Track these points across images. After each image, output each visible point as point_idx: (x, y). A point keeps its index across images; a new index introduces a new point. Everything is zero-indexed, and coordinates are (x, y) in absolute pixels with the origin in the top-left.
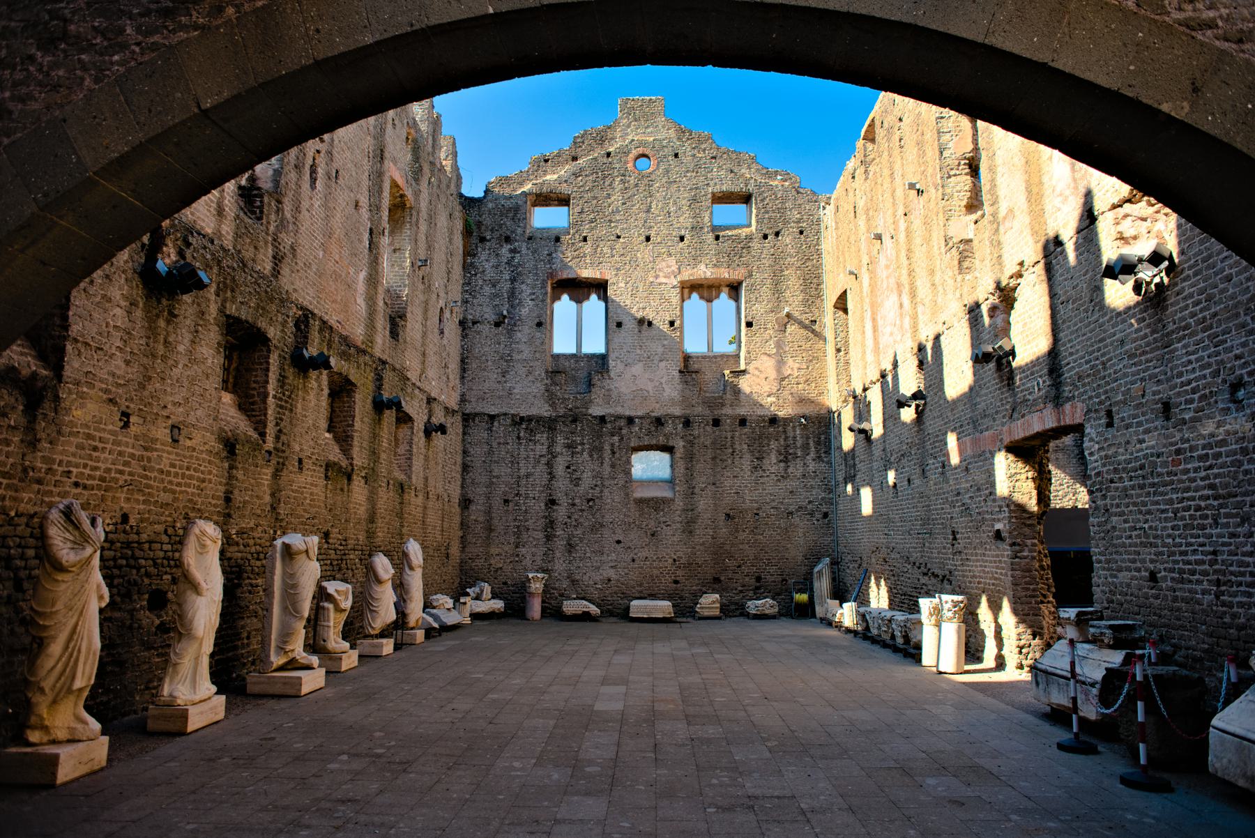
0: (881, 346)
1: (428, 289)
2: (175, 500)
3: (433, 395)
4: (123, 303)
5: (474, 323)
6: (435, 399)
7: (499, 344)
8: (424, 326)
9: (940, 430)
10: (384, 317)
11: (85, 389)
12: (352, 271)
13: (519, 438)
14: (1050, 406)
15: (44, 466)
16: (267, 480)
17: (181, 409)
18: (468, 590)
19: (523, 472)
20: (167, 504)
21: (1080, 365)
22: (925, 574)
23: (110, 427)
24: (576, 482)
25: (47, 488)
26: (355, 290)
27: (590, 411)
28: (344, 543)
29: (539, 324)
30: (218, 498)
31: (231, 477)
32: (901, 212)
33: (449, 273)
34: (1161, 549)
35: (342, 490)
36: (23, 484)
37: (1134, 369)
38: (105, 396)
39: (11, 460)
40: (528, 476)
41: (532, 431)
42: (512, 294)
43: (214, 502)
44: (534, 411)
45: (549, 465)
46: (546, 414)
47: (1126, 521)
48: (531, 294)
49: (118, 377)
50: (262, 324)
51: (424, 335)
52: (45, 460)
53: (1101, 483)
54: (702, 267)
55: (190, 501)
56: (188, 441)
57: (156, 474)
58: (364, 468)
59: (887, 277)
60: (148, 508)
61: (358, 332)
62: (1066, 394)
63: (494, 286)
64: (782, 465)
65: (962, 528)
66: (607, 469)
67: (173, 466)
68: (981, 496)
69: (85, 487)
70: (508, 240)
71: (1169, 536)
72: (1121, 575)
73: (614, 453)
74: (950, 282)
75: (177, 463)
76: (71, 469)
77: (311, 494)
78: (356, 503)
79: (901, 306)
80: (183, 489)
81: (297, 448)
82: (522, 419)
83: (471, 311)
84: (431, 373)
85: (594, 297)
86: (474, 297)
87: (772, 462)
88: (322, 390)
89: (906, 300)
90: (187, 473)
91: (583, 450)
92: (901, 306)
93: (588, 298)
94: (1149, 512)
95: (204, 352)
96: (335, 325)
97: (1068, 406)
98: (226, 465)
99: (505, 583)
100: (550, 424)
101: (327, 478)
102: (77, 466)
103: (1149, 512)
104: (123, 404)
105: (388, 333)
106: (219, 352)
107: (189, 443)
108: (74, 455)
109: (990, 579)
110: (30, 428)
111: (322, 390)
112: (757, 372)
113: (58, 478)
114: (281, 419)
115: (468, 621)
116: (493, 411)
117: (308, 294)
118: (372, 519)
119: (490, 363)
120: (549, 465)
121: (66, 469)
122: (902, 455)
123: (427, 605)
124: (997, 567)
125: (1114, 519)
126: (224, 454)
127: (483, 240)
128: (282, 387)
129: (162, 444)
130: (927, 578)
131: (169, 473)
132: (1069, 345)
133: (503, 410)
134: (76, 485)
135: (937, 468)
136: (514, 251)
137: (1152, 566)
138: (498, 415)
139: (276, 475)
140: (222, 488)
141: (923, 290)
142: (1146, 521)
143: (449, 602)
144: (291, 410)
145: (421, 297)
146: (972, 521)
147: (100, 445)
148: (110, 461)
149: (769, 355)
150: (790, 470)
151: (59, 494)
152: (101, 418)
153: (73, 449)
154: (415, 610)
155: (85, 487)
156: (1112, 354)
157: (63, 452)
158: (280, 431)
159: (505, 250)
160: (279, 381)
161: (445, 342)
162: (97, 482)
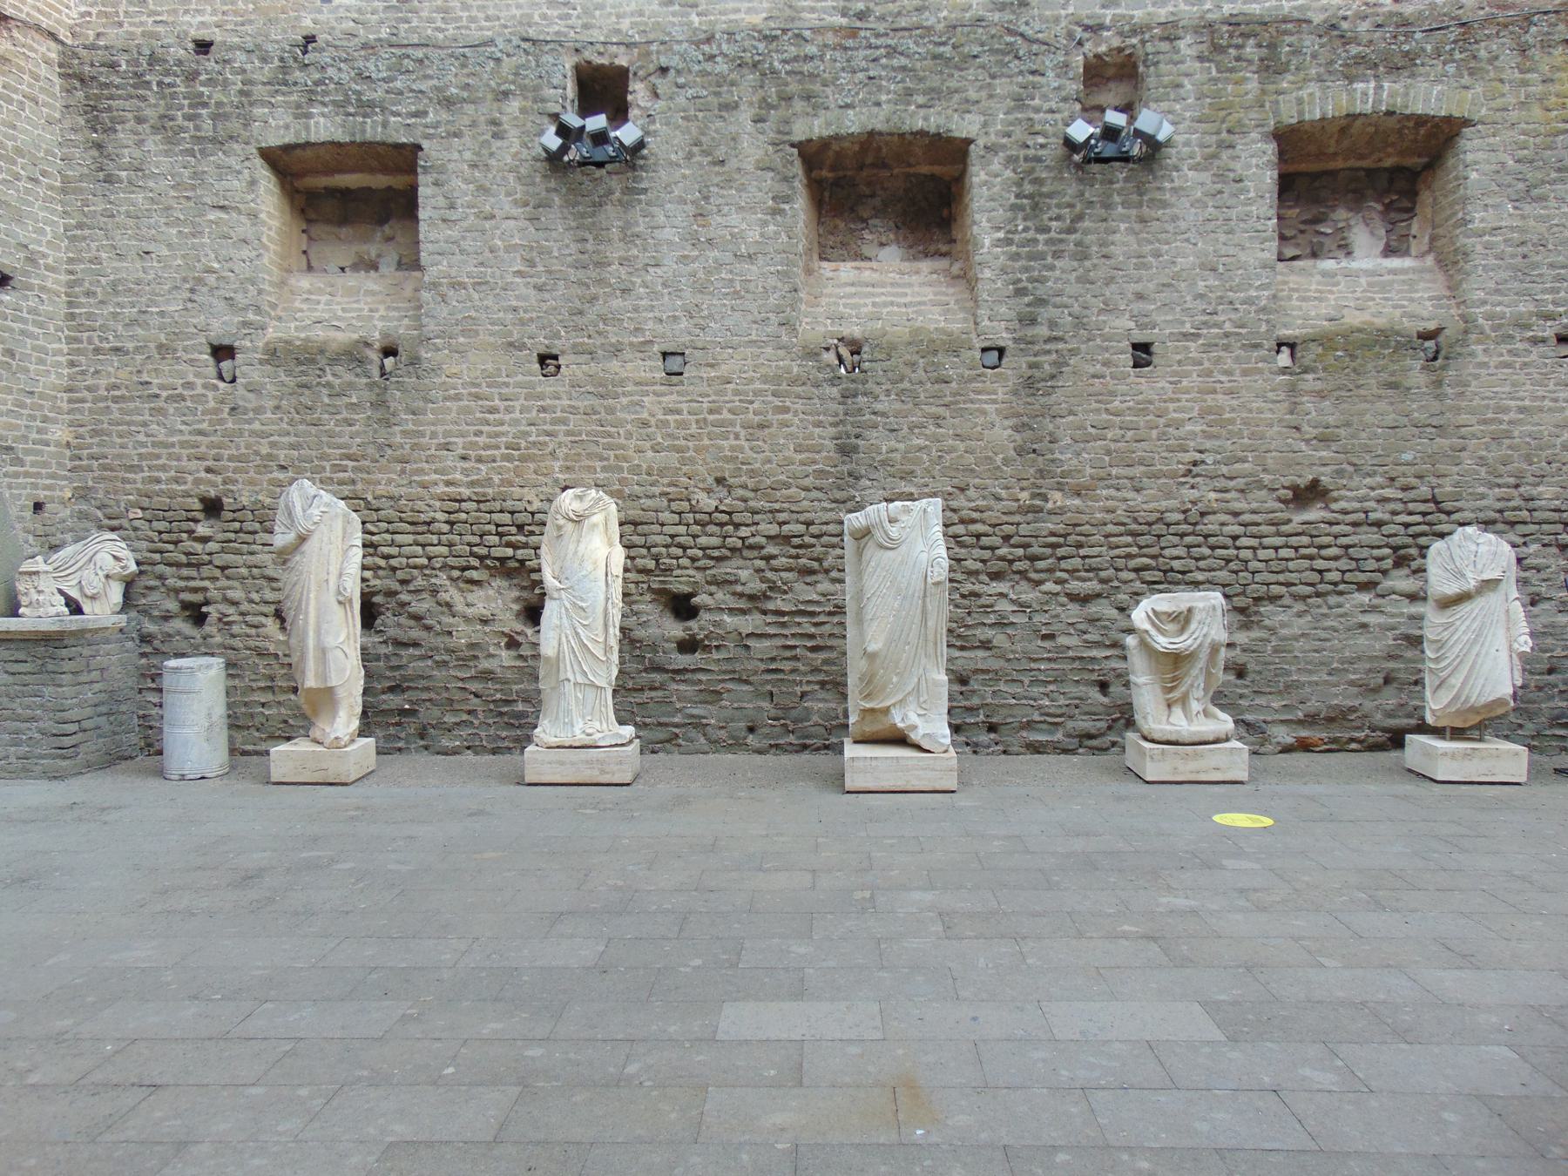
4: (517, 211)
11: (461, 340)
23: (520, 378)
57: (629, 427)
69: (479, 460)
75: (684, 406)
80: (706, 442)
104: (541, 343)
110: (380, 404)
121: (443, 441)
129: (637, 384)
148: (524, 422)
151: (436, 472)
162: (503, 451)
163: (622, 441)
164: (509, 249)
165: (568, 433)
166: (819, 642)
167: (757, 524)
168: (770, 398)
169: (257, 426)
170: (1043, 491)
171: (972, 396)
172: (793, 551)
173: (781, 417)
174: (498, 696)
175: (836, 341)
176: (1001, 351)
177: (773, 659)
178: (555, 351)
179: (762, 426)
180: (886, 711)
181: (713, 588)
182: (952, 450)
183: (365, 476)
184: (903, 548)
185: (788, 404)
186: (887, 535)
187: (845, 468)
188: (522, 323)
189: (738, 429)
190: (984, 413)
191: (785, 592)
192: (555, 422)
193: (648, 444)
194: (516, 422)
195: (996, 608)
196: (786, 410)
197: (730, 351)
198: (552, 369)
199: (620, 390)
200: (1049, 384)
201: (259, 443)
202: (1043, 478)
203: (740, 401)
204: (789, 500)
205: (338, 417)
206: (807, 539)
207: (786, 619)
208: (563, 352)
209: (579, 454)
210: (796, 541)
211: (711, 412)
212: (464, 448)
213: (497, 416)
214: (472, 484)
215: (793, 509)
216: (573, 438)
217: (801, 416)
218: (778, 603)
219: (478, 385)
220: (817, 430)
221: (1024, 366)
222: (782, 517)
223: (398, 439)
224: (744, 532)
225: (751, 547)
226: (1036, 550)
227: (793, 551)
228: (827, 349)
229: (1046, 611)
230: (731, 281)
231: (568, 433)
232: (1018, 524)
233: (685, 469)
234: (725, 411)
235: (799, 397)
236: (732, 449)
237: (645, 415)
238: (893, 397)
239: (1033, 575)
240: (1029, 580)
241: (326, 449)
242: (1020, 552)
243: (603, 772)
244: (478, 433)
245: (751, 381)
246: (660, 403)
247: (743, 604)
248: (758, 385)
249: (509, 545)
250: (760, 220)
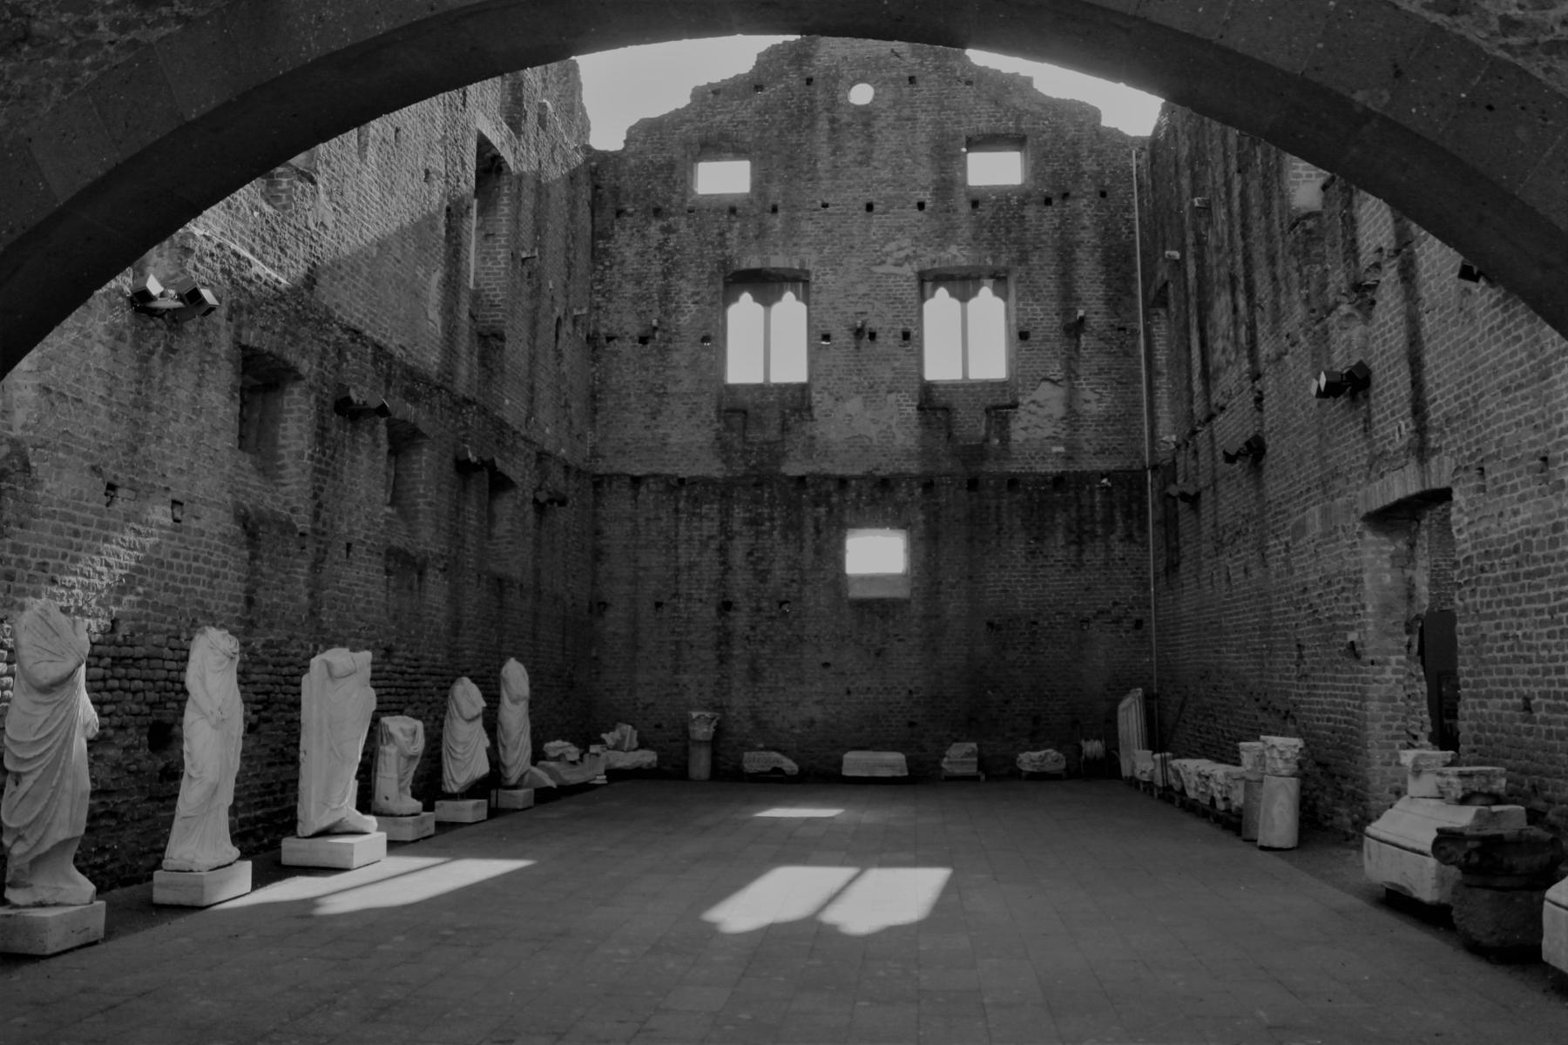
0: (1211, 369)
1: (537, 292)
2: (182, 601)
3: (547, 448)
5: (609, 339)
6: (548, 454)
7: (647, 369)
8: (532, 346)
9: (1283, 496)
10: (471, 335)
11: (61, 455)
12: (420, 272)
13: (677, 510)
14: (1413, 461)
15: (14, 556)
16: (303, 574)
17: (185, 478)
18: (604, 736)
19: (683, 561)
20: (170, 607)
21: (1448, 403)
22: (1265, 709)
23: (92, 504)
24: (762, 576)
25: (18, 585)
26: (426, 301)
27: (784, 469)
28: (414, 663)
29: (705, 339)
30: (237, 599)
31: (254, 571)
32: (1233, 166)
33: (569, 265)
34: (1535, 665)
35: (410, 588)
37: (1509, 409)
38: (86, 464)
40: (691, 566)
41: (696, 499)
42: (665, 295)
43: (231, 604)
44: (698, 471)
45: (722, 550)
46: (716, 474)
47: (1498, 627)
48: (694, 294)
49: (103, 438)
50: (291, 356)
51: (533, 359)
53: (1470, 572)
54: (953, 249)
55: (200, 603)
56: (194, 521)
58: (443, 557)
59: (1218, 266)
60: (145, 612)
61: (432, 360)
62: (1432, 444)
63: (639, 283)
64: (1073, 548)
65: (1310, 640)
66: (808, 557)
67: (176, 555)
68: (1331, 592)
70: (657, 212)
71: (1545, 646)
72: (1489, 702)
73: (818, 531)
74: (1295, 275)
75: (181, 551)
76: (47, 560)
77: (367, 594)
78: (431, 607)
79: (1235, 310)
80: (190, 586)
81: (344, 529)
82: (682, 481)
83: (605, 322)
84: (544, 415)
85: (789, 297)
86: (610, 300)
87: (1057, 545)
88: (378, 446)
89: (1242, 303)
90: (195, 565)
91: (773, 528)
92: (1235, 310)
93: (779, 298)
94: (1523, 614)
95: (213, 398)
96: (398, 353)
97: (1433, 461)
98: (246, 553)
99: (658, 726)
100: (724, 490)
101: (388, 572)
102: (54, 556)
103: (1523, 614)
104: (109, 471)
105: (475, 359)
106: (233, 398)
107: (194, 524)
109: (1342, 713)
111: (378, 446)
112: (1033, 407)
113: (31, 572)
114: (321, 489)
115: (601, 779)
116: (638, 470)
117: (357, 310)
118: (456, 627)
119: (633, 399)
120: (722, 550)
121: (41, 560)
122: (1238, 533)
123: (538, 756)
124: (1350, 697)
125: (1484, 624)
126: (243, 538)
127: (619, 213)
128: (321, 444)
130: (1265, 714)
131: (170, 566)
132: (1435, 373)
133: (655, 469)
135: (1279, 553)
136: (667, 230)
137: (1525, 690)
138: (647, 477)
139: (316, 566)
140: (242, 586)
141: (1263, 289)
142: (1520, 626)
143: (573, 752)
144: (335, 477)
145: (526, 304)
146: (1321, 630)
147: (82, 529)
149: (1053, 382)
150: (1085, 557)
152: (81, 492)
153: (48, 534)
154: (518, 757)
156: (1484, 388)
157: (39, 540)
158: (320, 505)
159: (654, 229)
160: (317, 435)
161: (565, 368)
164: (99, 370)
178: (118, 483)
179: (216, 576)
187: (249, 617)
188: (103, 448)
219: (67, 505)
237: (161, 556)
248: (216, 541)
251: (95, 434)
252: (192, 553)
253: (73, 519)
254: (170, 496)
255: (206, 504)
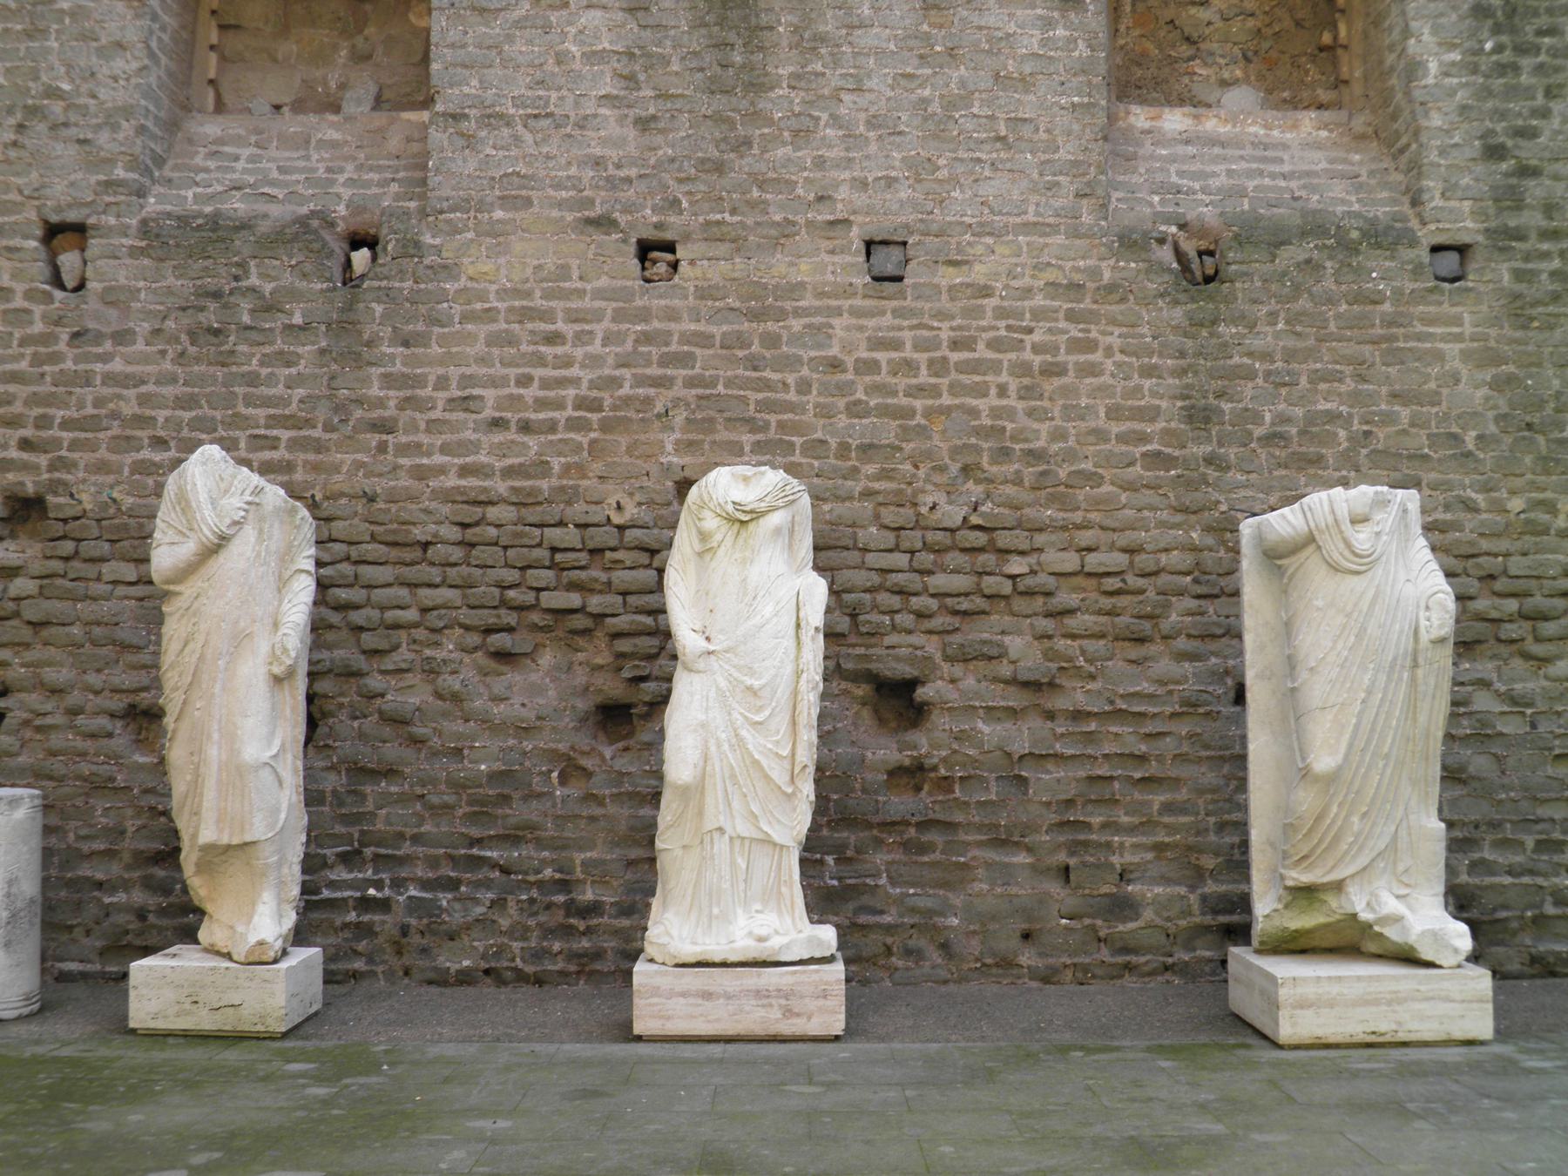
11: (499, 214)
15: (391, 393)
23: (603, 282)
36: (335, 436)
39: (300, 392)
49: (618, 166)
52: (389, 380)
57: (805, 371)
67: (878, 344)
69: (526, 427)
75: (907, 335)
76: (476, 392)
80: (947, 400)
102: (494, 383)
104: (647, 222)
107: (948, 277)
108: (483, 360)
110: (345, 325)
113: (437, 414)
129: (821, 295)
131: (871, 366)
134: (497, 424)
147: (568, 329)
148: (611, 360)
151: (444, 449)
153: (480, 347)
155: (526, 427)
162: (569, 412)
163: (792, 396)
164: (592, 57)
165: (690, 383)
166: (1153, 769)
167: (1040, 550)
168: (1062, 324)
169: (117, 366)
170: (1549, 495)
171: (1419, 328)
172: (1106, 602)
173: (1082, 358)
174: (548, 872)
175: (1174, 229)
176: (1462, 250)
177: (1070, 803)
178: (668, 236)
179: (1051, 371)
180: (1338, 886)
181: (958, 670)
182: (1389, 419)
183: (311, 457)
184: (1379, 571)
185: (1094, 335)
186: (1348, 545)
188: (612, 184)
189: (1004, 378)
190: (1439, 356)
191: (1092, 677)
192: (665, 361)
193: (841, 403)
194: (594, 361)
195: (1475, 708)
196: (1091, 346)
197: (989, 240)
198: (662, 268)
199: (788, 305)
200: (1551, 309)
201: (119, 397)
202: (1547, 472)
203: (1009, 328)
204: (1097, 504)
205: (267, 350)
206: (1133, 581)
207: (1093, 726)
208: (687, 237)
209: (711, 420)
210: (1112, 583)
211: (955, 345)
212: (498, 408)
213: (559, 350)
214: (509, 472)
215: (1108, 522)
216: (700, 391)
217: (1119, 357)
218: (1076, 696)
219: (528, 294)
220: (1147, 383)
221: (1506, 277)
222: (1085, 538)
223: (375, 391)
224: (1017, 566)
225: (1029, 593)
226: (1538, 601)
227: (1106, 602)
228: (1161, 241)
229: (1559, 714)
230: (992, 118)
231: (690, 383)
232: (1507, 555)
233: (908, 447)
234: (981, 346)
235: (1113, 322)
236: (996, 413)
237: (834, 351)
238: (1280, 326)
239: (1539, 649)
240: (1527, 656)
241: (242, 409)
242: (1512, 605)
243: (788, 1012)
244: (524, 381)
245: (1028, 292)
246: (861, 328)
247: (1015, 698)
248: (1039, 301)
249: (573, 586)
250: (1040, 17)
251: (598, 163)
252: (945, 335)
253: (546, 316)
254: (856, 236)
255: (983, 230)
